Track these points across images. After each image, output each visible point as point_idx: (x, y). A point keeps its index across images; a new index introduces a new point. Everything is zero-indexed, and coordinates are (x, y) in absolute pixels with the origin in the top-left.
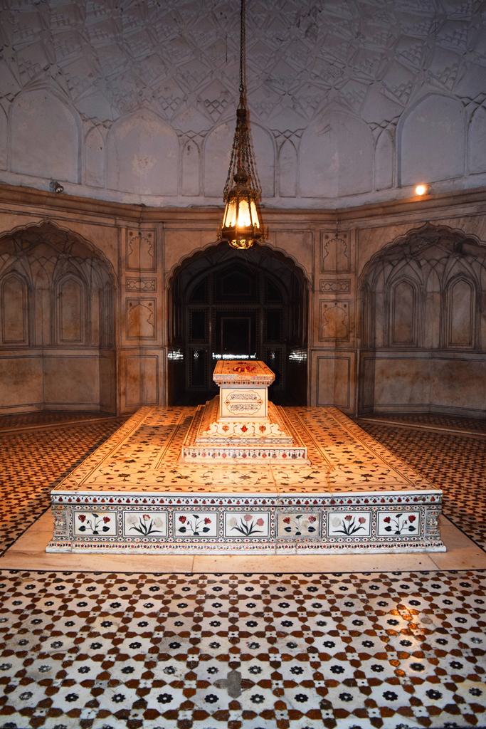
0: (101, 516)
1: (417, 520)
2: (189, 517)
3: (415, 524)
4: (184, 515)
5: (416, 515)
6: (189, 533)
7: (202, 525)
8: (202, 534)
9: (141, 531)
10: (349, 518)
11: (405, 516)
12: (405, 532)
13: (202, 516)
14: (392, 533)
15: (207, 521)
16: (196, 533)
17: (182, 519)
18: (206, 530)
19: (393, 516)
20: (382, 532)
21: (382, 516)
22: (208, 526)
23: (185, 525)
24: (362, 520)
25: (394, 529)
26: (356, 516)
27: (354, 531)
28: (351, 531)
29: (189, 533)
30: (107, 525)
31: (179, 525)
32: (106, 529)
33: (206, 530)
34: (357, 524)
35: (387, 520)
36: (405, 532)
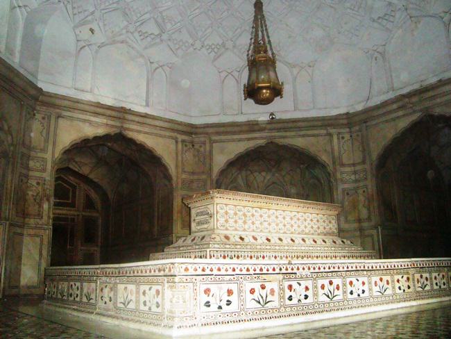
0: (304, 283)
6: (355, 295)
10: (421, 277)
12: (443, 287)
16: (359, 295)
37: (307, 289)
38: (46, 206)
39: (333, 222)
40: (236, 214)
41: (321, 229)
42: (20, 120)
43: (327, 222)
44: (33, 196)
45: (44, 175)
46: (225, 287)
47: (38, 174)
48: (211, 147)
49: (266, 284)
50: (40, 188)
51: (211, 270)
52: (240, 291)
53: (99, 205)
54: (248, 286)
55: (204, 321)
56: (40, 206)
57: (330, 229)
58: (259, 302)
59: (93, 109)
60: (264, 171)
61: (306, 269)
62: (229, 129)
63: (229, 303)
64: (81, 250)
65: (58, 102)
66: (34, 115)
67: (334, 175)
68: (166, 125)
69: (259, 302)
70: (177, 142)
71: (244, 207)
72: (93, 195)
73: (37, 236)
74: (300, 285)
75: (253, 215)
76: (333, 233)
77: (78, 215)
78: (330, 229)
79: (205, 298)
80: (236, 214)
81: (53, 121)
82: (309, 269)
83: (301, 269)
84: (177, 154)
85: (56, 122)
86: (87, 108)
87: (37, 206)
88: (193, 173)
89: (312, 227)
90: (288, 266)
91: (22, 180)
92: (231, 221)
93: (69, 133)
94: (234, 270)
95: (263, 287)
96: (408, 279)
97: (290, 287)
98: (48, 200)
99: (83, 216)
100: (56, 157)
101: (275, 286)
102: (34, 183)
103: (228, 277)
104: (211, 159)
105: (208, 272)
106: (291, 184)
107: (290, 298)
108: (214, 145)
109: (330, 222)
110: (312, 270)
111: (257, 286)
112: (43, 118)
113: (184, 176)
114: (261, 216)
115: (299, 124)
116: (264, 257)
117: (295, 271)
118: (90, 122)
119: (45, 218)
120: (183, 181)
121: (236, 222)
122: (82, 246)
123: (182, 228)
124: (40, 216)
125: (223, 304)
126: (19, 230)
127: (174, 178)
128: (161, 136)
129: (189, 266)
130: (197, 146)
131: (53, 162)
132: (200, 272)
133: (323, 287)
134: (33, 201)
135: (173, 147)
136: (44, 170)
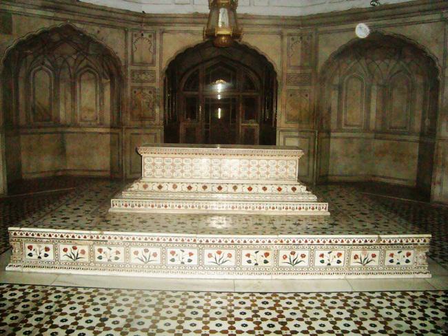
0: (114, 249)
1: (343, 255)
2: (178, 251)
3: (341, 259)
4: (174, 250)
5: (343, 252)
6: (178, 262)
7: (187, 257)
8: (186, 263)
9: (142, 260)
10: (293, 253)
11: (335, 253)
12: (334, 264)
13: (187, 251)
14: (325, 264)
15: (191, 254)
17: (173, 253)
18: (190, 261)
19: (326, 253)
20: (318, 263)
21: (318, 253)
22: (191, 258)
23: (174, 257)
24: (303, 256)
25: (326, 262)
26: (299, 253)
27: (296, 263)
28: (295, 262)
29: (178, 262)
30: (118, 256)
31: (170, 257)
32: (117, 258)
33: (190, 261)
34: (300, 258)
35: (322, 255)
36: (334, 264)
37: (118, 252)
38: (157, 110)
39: (292, 167)
40: (163, 164)
41: (273, 174)
42: (126, 47)
43: (282, 167)
44: (146, 102)
45: (154, 85)
46: (44, 246)
47: (149, 85)
48: (317, 40)
49: (77, 246)
50: (152, 95)
51: (33, 235)
52: (55, 249)
53: (258, 85)
54: (62, 247)
55: (27, 264)
56: (153, 109)
57: (286, 173)
58: (71, 257)
59: (189, 20)
60: (386, 58)
61: (118, 239)
62: (331, 19)
63: (46, 255)
64: (242, 126)
65: (160, 20)
66: (142, 35)
67: (442, 72)
68: (268, 22)
69: (71, 257)
70: (282, 37)
71: (173, 158)
72: (252, 75)
73: (151, 134)
74: (110, 249)
75: (182, 165)
76: (290, 178)
77: (239, 96)
78: (286, 173)
79: (28, 251)
80: (163, 164)
81: (158, 35)
82: (122, 238)
83: (113, 239)
84: (282, 50)
85: (161, 40)
86: (185, 20)
87: (151, 111)
88: (301, 67)
89: (258, 173)
90: (99, 236)
91: (135, 92)
92: (158, 171)
93: (172, 45)
94: (50, 236)
95: (75, 248)
96: (267, 255)
97: (100, 250)
98: (159, 105)
99: (243, 96)
100: (165, 66)
101: (86, 248)
102: (147, 92)
103: (45, 240)
104: (317, 52)
105: (30, 236)
106: (417, 73)
107: (100, 258)
108: (321, 37)
109: (286, 167)
110: (125, 240)
111: (69, 247)
112: (150, 36)
113: (290, 71)
114: (192, 165)
115: (410, 9)
116: (166, 207)
117: (106, 239)
118: (192, 33)
119: (157, 120)
120: (288, 76)
121: (163, 171)
122: (242, 122)
123: (286, 123)
124: (153, 118)
125: (42, 255)
126: (136, 131)
127: (279, 74)
128: (263, 33)
129: (17, 233)
130: (305, 38)
131: (161, 72)
132: (24, 235)
133: (136, 253)
134: (147, 106)
135: (276, 41)
136: (153, 81)
